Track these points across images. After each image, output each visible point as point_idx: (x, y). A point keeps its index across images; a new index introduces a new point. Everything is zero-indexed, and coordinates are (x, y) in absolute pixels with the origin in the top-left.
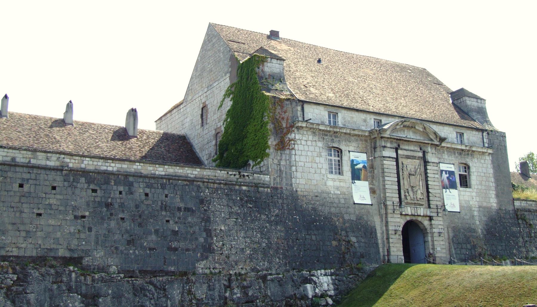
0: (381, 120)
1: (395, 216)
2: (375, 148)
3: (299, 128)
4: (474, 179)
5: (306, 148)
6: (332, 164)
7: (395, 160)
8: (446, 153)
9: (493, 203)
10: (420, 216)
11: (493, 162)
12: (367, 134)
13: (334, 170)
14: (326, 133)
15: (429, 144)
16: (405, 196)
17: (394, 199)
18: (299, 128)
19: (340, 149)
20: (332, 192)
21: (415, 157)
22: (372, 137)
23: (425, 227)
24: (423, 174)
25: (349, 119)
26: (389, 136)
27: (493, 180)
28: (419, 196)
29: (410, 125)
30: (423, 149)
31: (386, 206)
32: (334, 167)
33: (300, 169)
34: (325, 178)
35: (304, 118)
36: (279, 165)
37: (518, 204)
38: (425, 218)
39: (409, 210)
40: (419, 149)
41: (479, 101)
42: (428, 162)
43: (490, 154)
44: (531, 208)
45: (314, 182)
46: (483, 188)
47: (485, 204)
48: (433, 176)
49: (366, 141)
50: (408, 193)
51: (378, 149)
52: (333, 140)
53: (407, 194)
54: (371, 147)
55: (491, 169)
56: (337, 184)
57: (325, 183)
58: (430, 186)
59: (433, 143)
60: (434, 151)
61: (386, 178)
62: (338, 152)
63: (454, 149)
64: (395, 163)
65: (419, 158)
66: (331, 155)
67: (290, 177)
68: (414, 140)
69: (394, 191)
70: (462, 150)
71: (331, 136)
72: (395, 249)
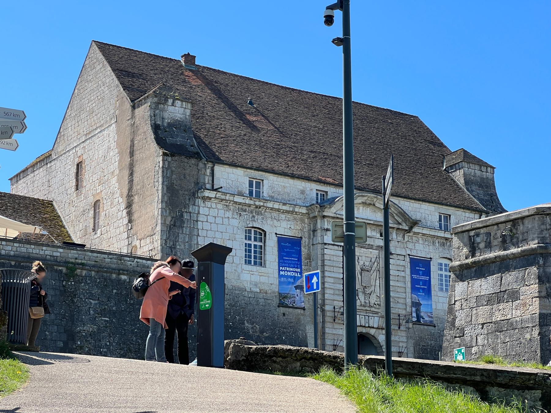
0: (327, 192)
1: (336, 326)
2: (314, 231)
3: (205, 199)
5: (214, 227)
6: (250, 251)
7: (341, 249)
8: (421, 242)
10: (373, 328)
12: (304, 211)
13: (253, 260)
14: (244, 208)
17: (336, 303)
18: (205, 199)
19: (263, 231)
20: (248, 290)
21: (372, 245)
22: (311, 215)
23: (379, 343)
24: (382, 270)
25: (280, 190)
26: (335, 215)
28: (373, 299)
29: (368, 202)
31: (323, 311)
32: (253, 254)
34: (239, 270)
35: (213, 186)
36: (175, 248)
38: (380, 331)
40: (378, 235)
41: (484, 169)
42: (392, 254)
48: (397, 273)
49: (302, 221)
51: (319, 233)
52: (254, 217)
54: (309, 230)
56: (255, 278)
57: (239, 276)
59: (400, 227)
60: (400, 238)
61: (327, 274)
62: (261, 234)
63: (434, 236)
66: (250, 239)
68: (372, 222)
69: (337, 292)
71: (252, 212)
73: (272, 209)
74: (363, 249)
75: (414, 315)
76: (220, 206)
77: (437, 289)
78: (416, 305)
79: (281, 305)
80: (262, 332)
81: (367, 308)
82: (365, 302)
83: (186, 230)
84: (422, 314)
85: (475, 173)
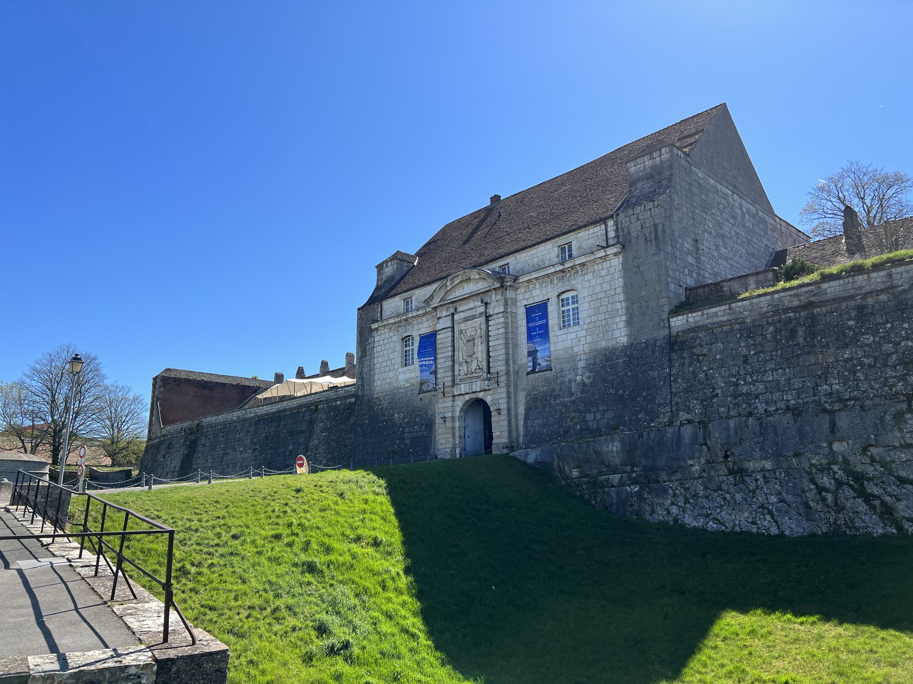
1: (446, 399)
4: (585, 309)
8: (538, 287)
9: (621, 336)
11: (624, 264)
15: (490, 291)
18: (377, 329)
27: (622, 297)
30: (487, 299)
33: (377, 371)
37: (679, 323)
39: (463, 388)
40: (480, 303)
42: (491, 316)
43: (615, 254)
44: (716, 320)
45: (388, 381)
46: (602, 317)
47: (603, 344)
55: (621, 280)
56: (407, 376)
63: (548, 275)
64: (450, 334)
65: (481, 314)
67: (372, 381)
70: (562, 271)
72: (443, 441)
73: (414, 317)
75: (531, 364)
76: (386, 331)
77: (556, 328)
78: (532, 354)
79: (421, 392)
80: (404, 419)
83: (368, 357)
84: (539, 361)
85: (645, 166)
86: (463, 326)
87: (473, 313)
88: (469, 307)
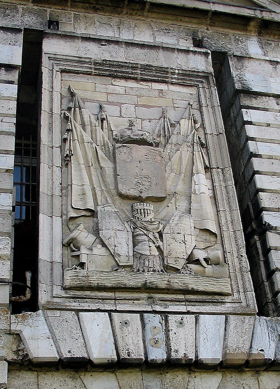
7: (15, 76)
16: (71, 245)
40: (187, 44)
50: (96, 231)
53: (84, 236)
58: (266, 200)
59: (267, 16)
74: (122, 83)
81: (150, 278)
82: (138, 256)
86: (87, 87)
87: (160, 60)
88: (126, 36)
